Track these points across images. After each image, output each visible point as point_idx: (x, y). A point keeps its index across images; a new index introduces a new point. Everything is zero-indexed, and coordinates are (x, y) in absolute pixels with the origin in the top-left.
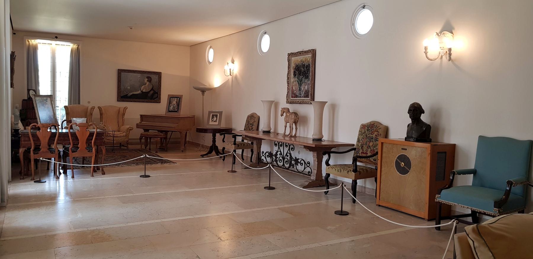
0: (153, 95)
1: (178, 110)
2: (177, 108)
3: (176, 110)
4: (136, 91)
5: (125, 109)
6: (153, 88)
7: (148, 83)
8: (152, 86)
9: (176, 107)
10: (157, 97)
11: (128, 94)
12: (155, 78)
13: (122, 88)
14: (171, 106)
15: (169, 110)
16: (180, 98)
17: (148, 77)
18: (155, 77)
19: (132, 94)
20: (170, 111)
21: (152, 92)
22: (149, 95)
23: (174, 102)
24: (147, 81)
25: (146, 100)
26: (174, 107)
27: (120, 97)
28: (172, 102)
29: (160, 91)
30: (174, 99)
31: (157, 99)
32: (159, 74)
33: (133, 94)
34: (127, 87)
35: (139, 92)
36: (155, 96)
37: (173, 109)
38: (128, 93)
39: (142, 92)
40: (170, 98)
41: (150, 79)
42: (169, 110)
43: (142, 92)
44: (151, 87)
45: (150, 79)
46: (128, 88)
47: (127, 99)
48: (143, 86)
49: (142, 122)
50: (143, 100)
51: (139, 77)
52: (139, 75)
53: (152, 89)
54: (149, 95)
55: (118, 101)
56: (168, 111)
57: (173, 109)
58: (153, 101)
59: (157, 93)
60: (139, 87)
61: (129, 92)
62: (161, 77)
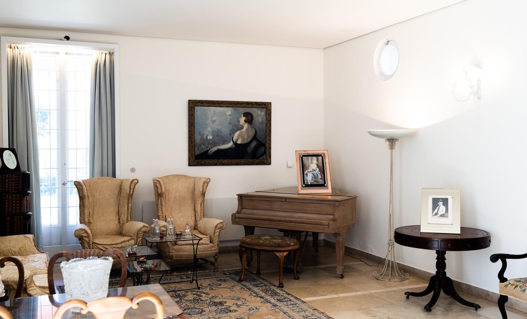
0: (256, 148)
1: (325, 183)
2: (321, 178)
3: (321, 182)
4: (225, 142)
5: (207, 182)
6: (257, 136)
7: (246, 126)
8: (254, 131)
9: (320, 177)
10: (265, 153)
11: (209, 150)
12: (259, 114)
13: (198, 137)
14: (307, 174)
15: (306, 183)
16: (322, 157)
17: (246, 114)
18: (259, 112)
19: (216, 149)
20: (307, 186)
21: (254, 144)
22: (250, 150)
23: (313, 165)
24: (246, 121)
25: (243, 161)
26: (315, 177)
27: (194, 157)
28: (307, 166)
29: (270, 140)
30: (311, 160)
31: (264, 157)
32: (266, 107)
33: (219, 151)
34: (207, 136)
35: (230, 145)
36: (260, 152)
37: (314, 179)
38: (208, 149)
39: (235, 143)
40: (302, 158)
41: (249, 119)
42: (306, 183)
43: (235, 143)
44: (252, 133)
45: (250, 118)
46: (209, 138)
47: (207, 161)
48: (238, 132)
49: (244, 211)
50: (237, 161)
51: (230, 115)
52: (229, 111)
53: (255, 138)
54: (250, 150)
55: (190, 165)
56: (304, 185)
57: (314, 179)
58: (257, 161)
59: (264, 145)
60: (230, 134)
61: (210, 146)
62: (271, 112)
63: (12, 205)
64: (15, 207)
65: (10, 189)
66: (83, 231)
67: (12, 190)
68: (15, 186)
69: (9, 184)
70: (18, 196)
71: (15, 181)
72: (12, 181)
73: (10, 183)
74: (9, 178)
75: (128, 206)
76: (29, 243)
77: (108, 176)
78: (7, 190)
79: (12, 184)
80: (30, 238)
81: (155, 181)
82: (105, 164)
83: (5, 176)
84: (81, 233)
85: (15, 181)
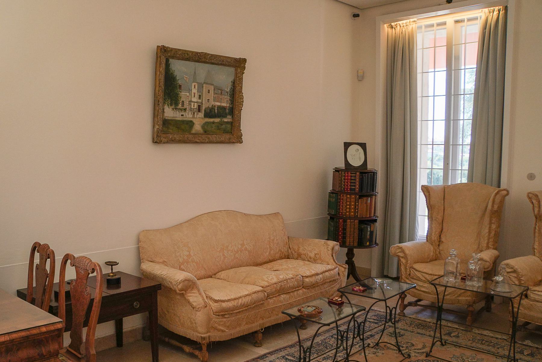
63: (346, 207)
64: (350, 208)
65: (346, 188)
66: (400, 250)
67: (347, 190)
68: (351, 186)
69: (344, 182)
70: (353, 197)
71: (351, 179)
72: (348, 179)
73: (346, 181)
74: (345, 176)
75: (490, 227)
76: (326, 250)
77: (485, 184)
78: (342, 189)
79: (347, 183)
80: (329, 245)
81: (530, 195)
82: (489, 166)
83: (342, 173)
84: (398, 251)
85: (351, 179)
